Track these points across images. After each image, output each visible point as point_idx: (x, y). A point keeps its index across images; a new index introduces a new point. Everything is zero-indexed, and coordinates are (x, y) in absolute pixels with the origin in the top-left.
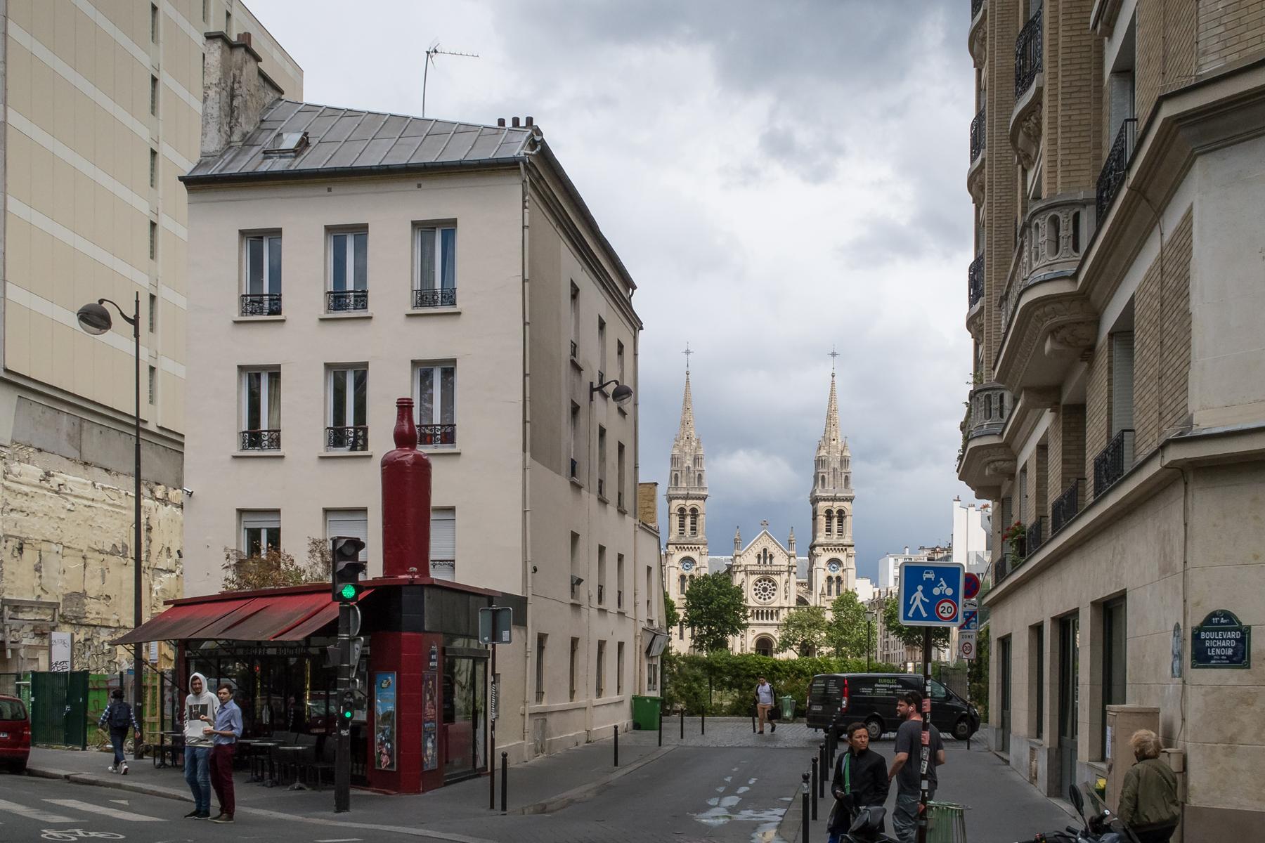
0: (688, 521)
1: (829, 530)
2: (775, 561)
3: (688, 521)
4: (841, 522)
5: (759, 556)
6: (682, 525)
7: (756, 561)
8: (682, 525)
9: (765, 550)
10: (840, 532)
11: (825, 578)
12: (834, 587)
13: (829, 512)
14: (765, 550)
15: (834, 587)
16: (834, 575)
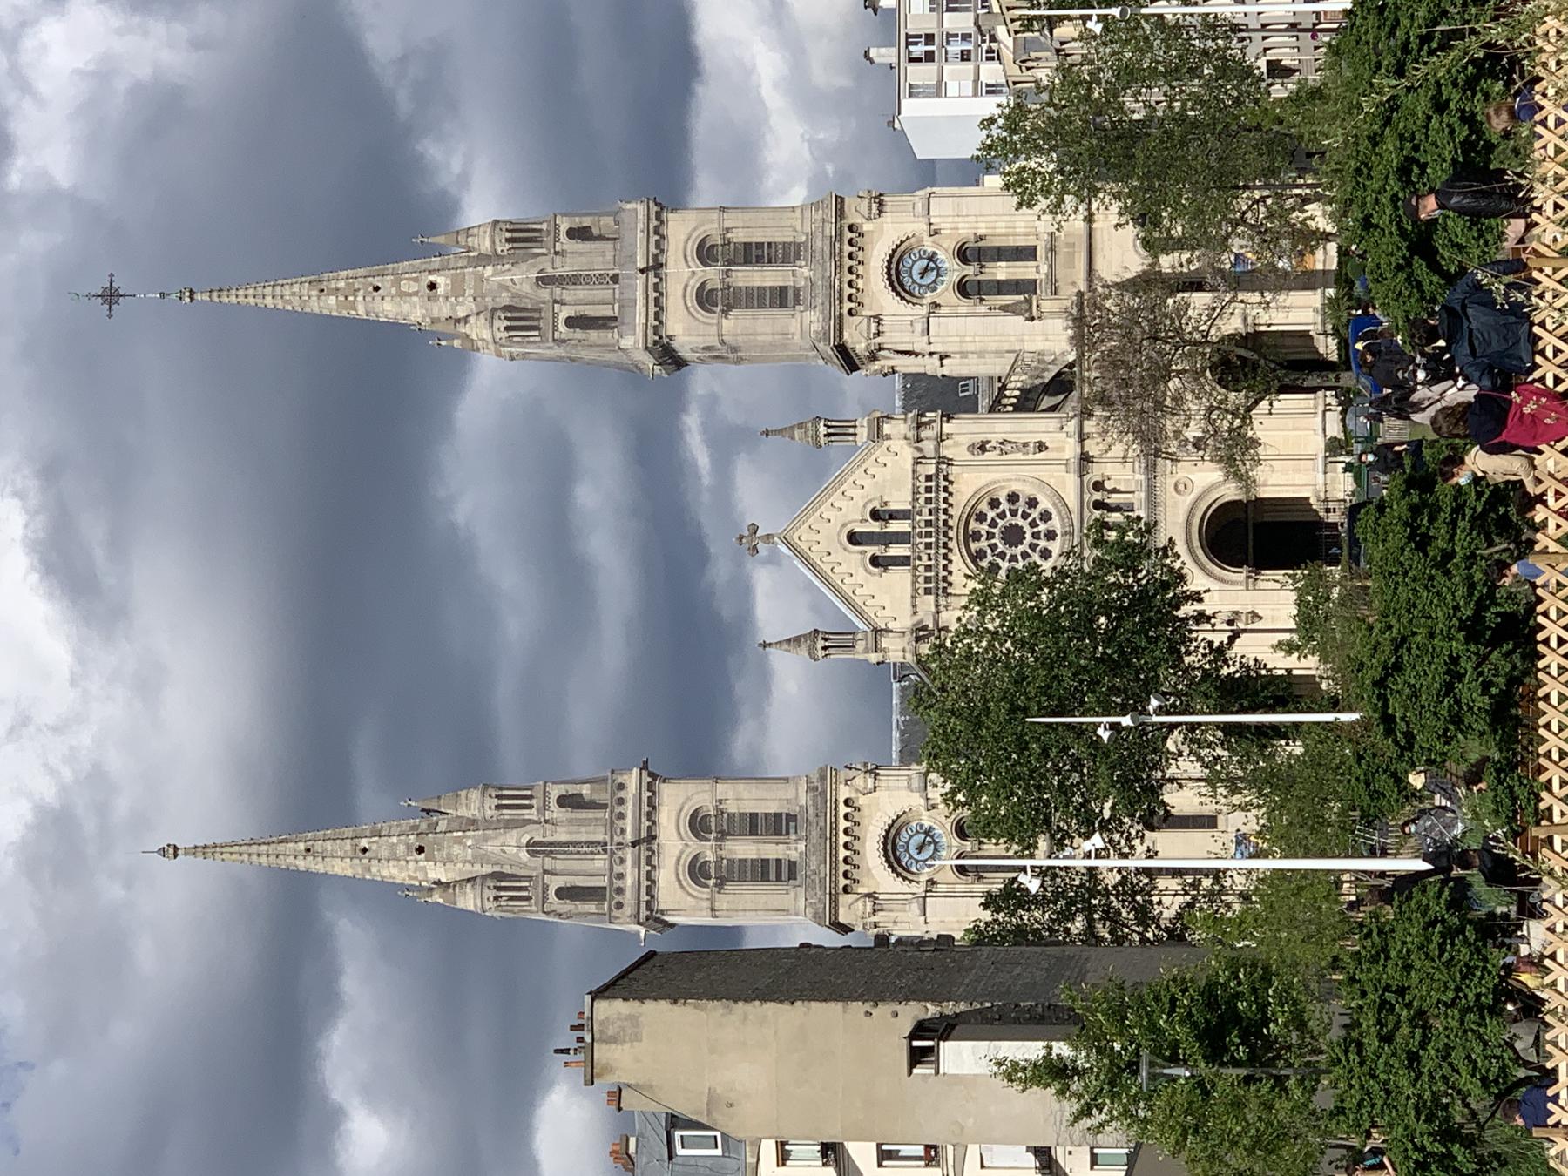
0: (744, 849)
1: (781, 298)
2: (900, 501)
3: (744, 849)
4: (753, 254)
5: (875, 561)
6: (763, 871)
7: (900, 575)
8: (763, 871)
9: (853, 538)
10: (788, 254)
11: (965, 306)
12: (1002, 271)
13: (705, 298)
14: (853, 538)
15: (1002, 271)
16: (955, 271)
